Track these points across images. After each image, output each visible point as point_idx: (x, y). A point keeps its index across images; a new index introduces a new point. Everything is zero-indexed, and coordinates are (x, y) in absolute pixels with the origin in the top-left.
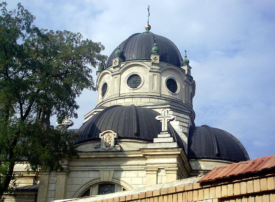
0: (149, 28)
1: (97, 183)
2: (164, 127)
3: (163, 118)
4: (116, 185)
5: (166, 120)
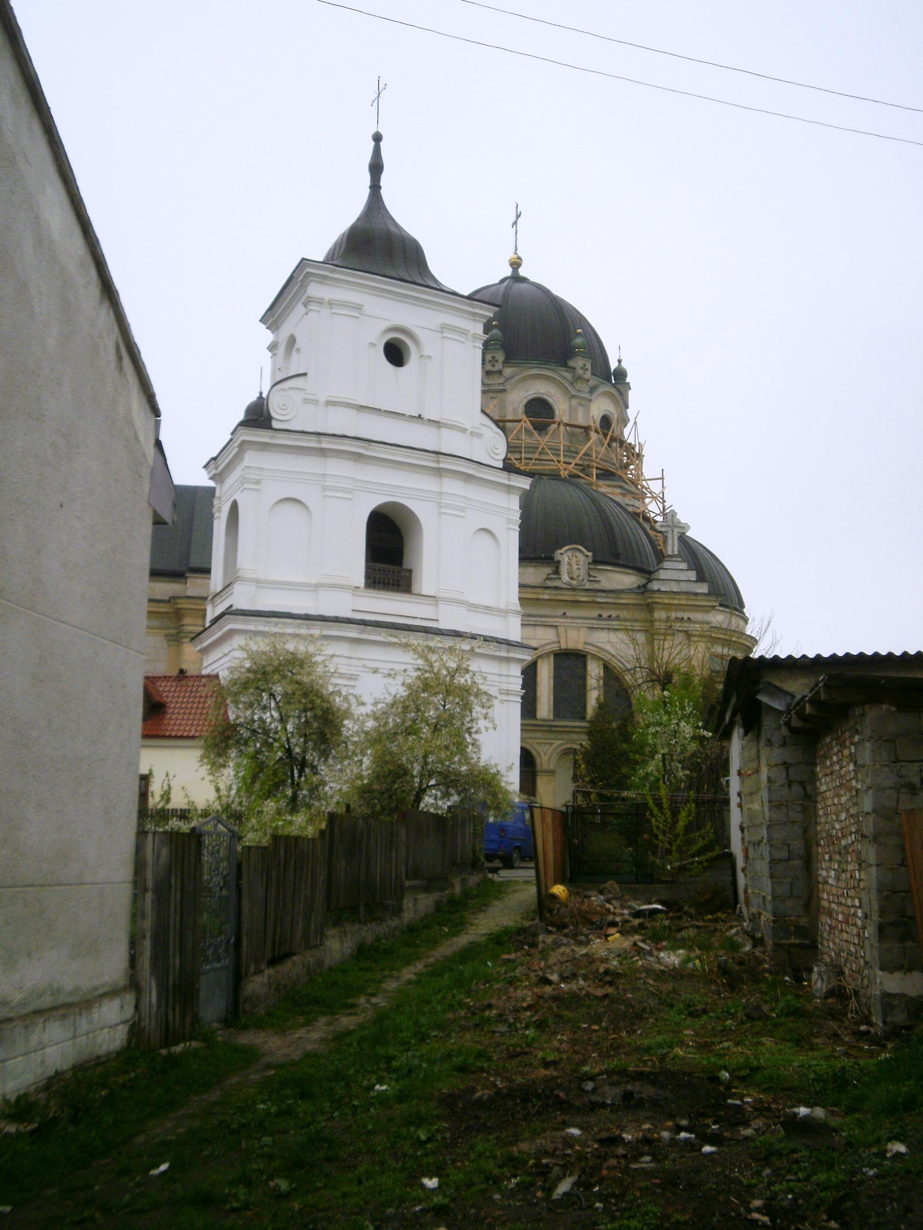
0: (516, 264)
1: (551, 652)
2: (672, 547)
3: (669, 529)
4: (589, 657)
5: (676, 533)
